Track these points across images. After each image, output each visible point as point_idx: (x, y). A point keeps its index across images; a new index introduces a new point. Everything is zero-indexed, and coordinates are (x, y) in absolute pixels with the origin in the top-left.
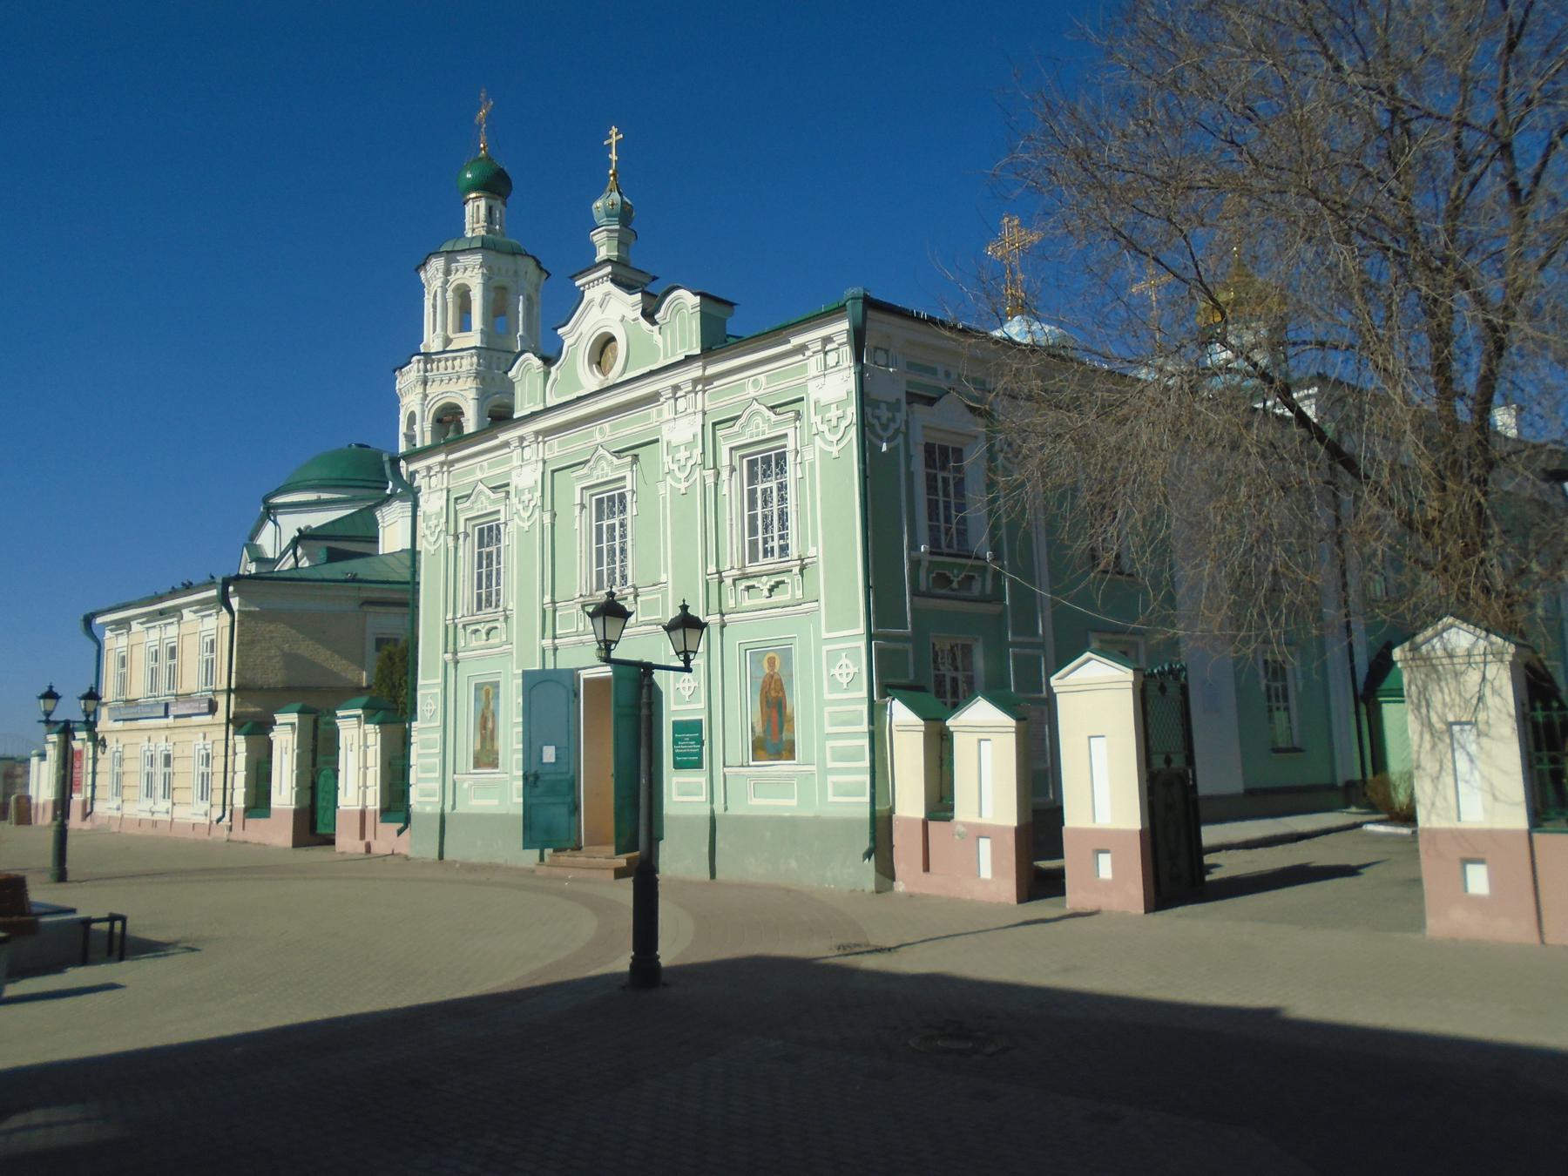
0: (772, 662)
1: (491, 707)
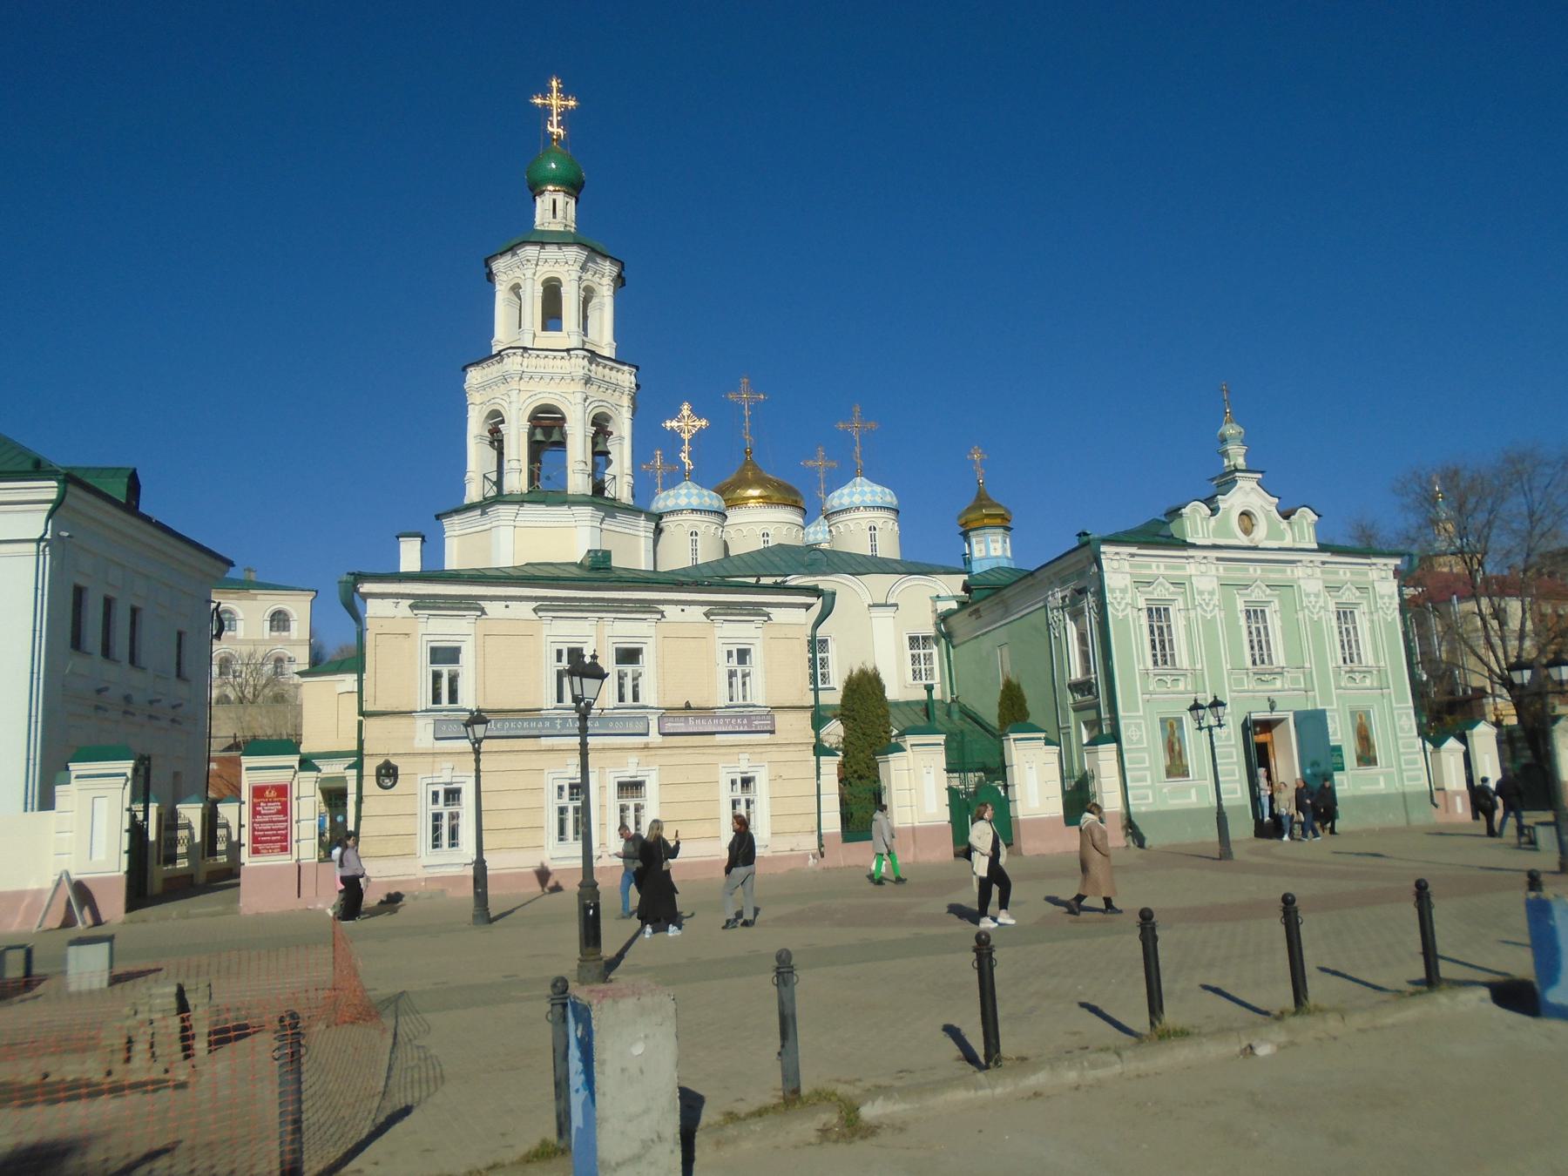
0: (1361, 717)
1: (1176, 735)
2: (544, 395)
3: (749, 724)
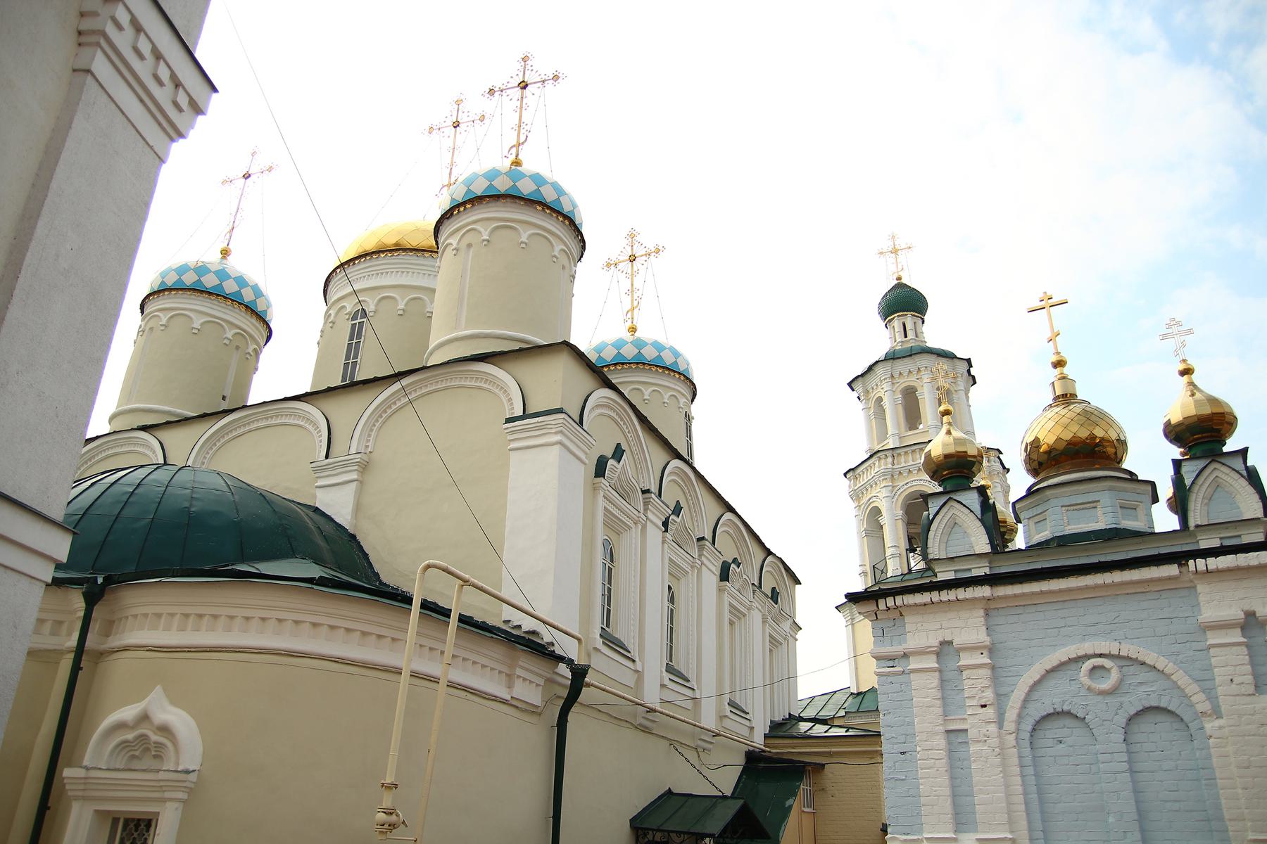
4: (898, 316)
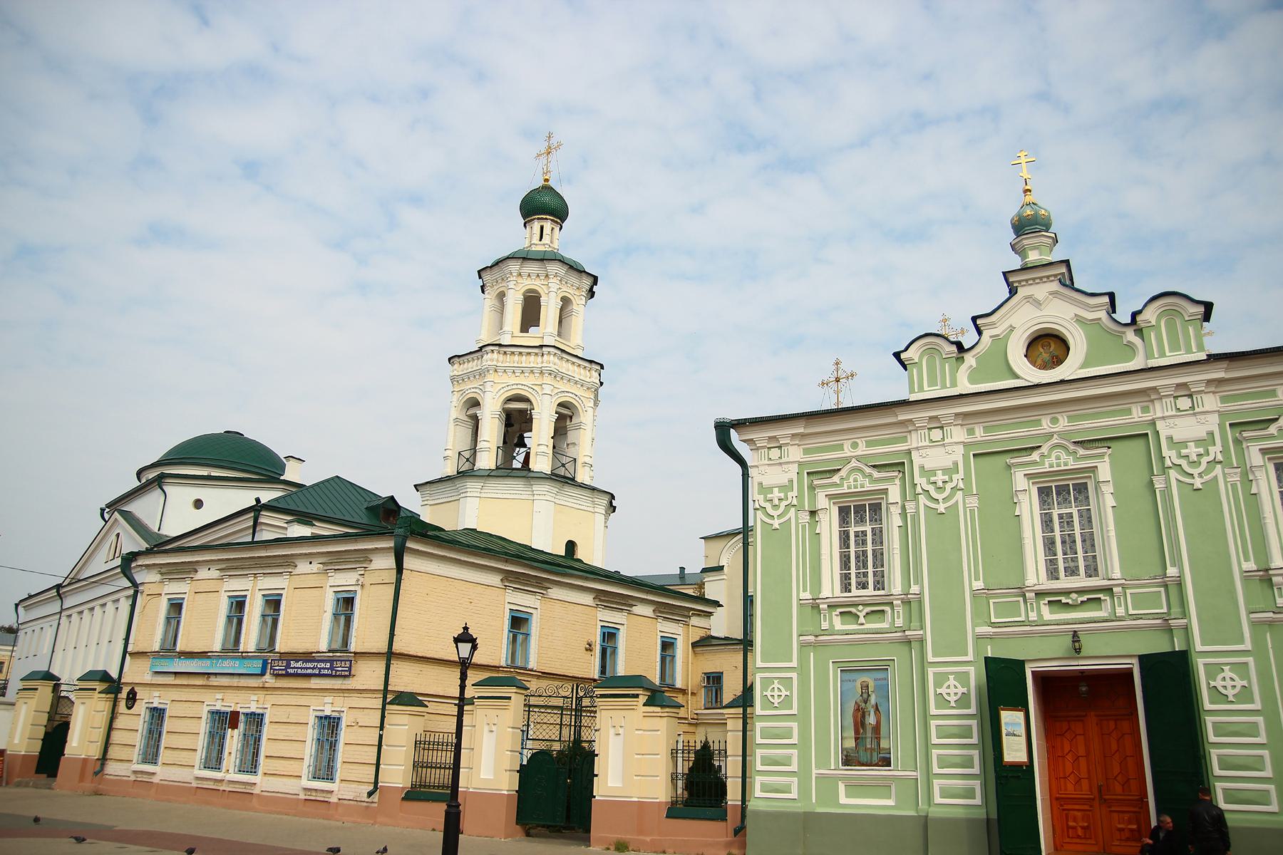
1: (873, 700)
2: (469, 391)
3: (332, 668)
4: (538, 219)
